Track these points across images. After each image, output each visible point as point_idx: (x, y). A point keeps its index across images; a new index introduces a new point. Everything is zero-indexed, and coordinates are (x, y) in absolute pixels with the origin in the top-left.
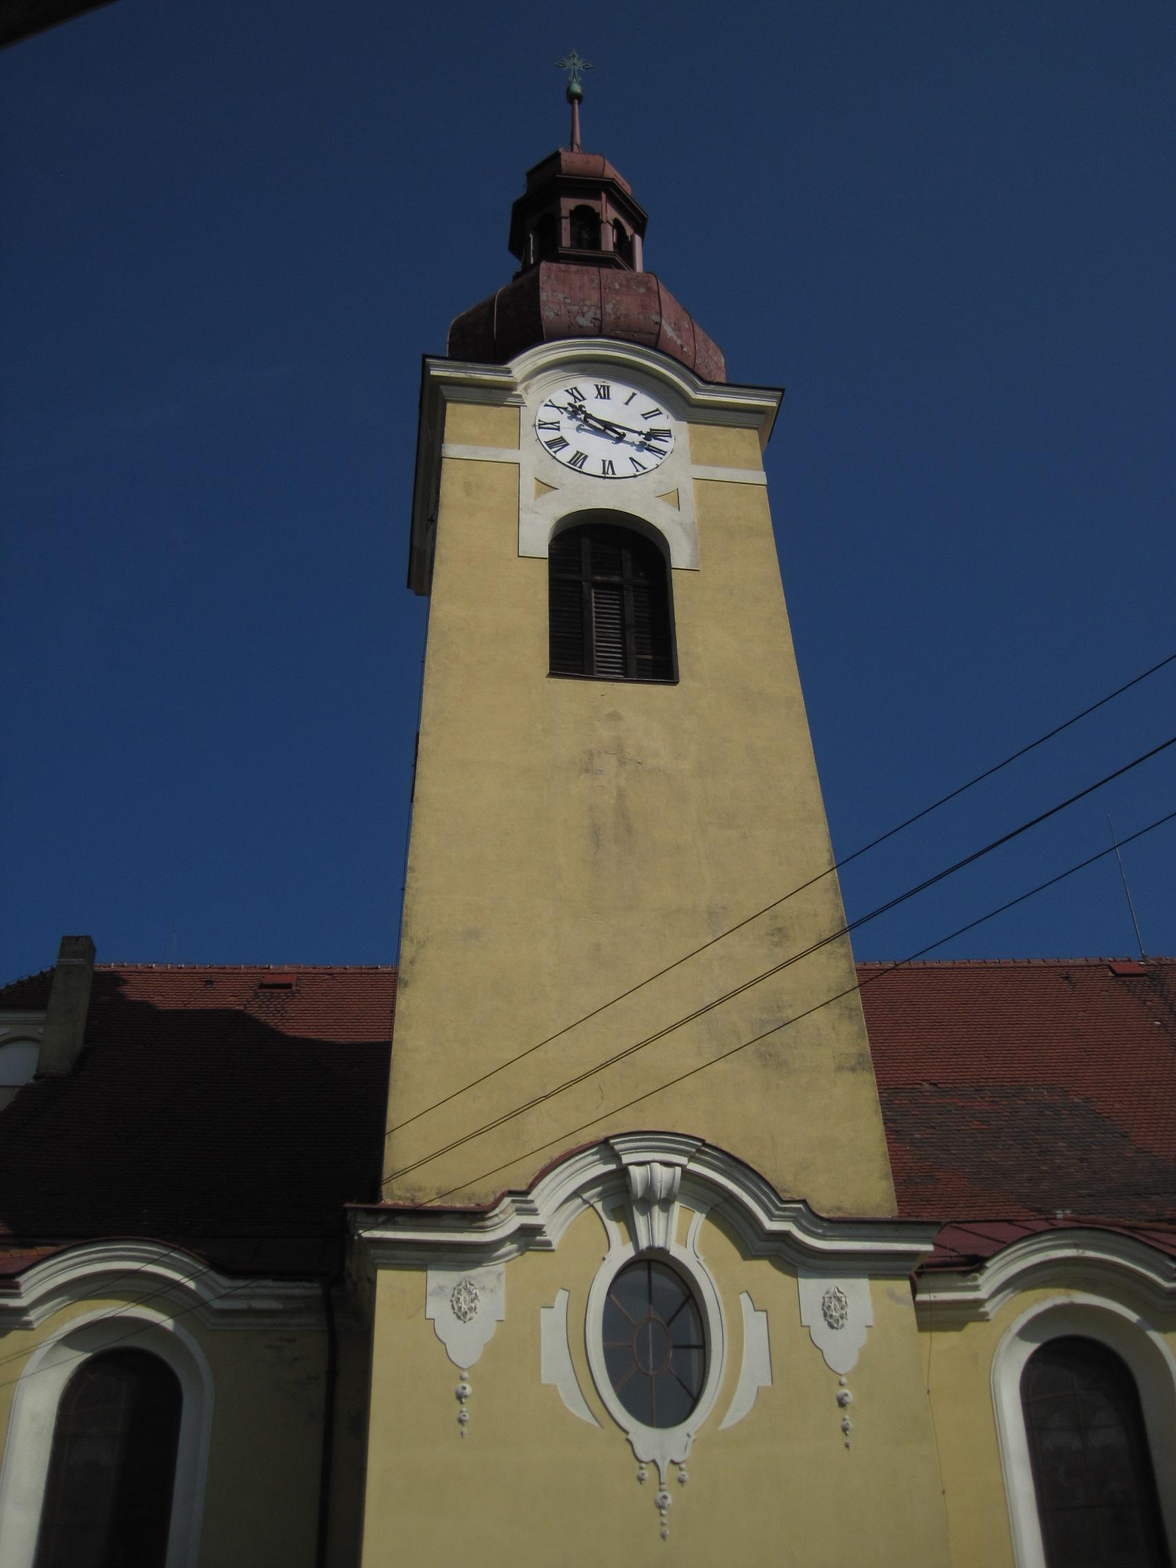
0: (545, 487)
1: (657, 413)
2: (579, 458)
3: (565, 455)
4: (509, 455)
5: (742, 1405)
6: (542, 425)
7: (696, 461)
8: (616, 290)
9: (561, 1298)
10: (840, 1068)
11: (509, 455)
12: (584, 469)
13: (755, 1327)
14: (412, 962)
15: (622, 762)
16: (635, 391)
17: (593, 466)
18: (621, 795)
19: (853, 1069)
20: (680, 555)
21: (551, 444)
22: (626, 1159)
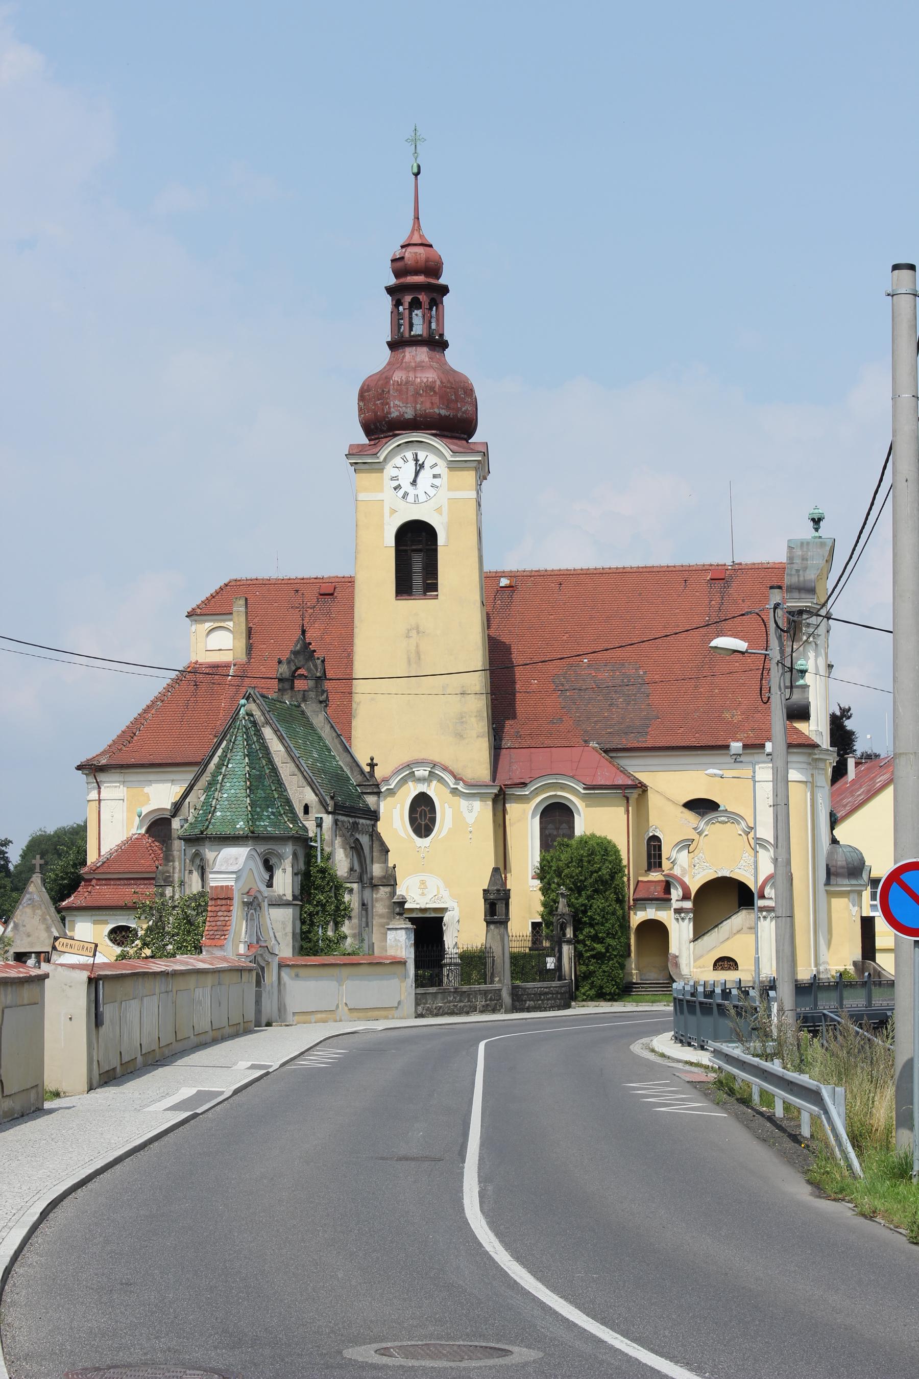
0: (393, 511)
1: (436, 465)
2: (406, 495)
3: (401, 493)
4: (379, 496)
5: (444, 832)
6: (393, 479)
7: (449, 489)
8: (420, 395)
9: (399, 805)
10: (478, 737)
11: (379, 496)
12: (407, 501)
13: (449, 812)
14: (356, 710)
15: (418, 633)
16: (428, 454)
17: (411, 498)
18: (417, 646)
19: (482, 737)
20: (441, 541)
21: (395, 489)
22: (414, 770)
